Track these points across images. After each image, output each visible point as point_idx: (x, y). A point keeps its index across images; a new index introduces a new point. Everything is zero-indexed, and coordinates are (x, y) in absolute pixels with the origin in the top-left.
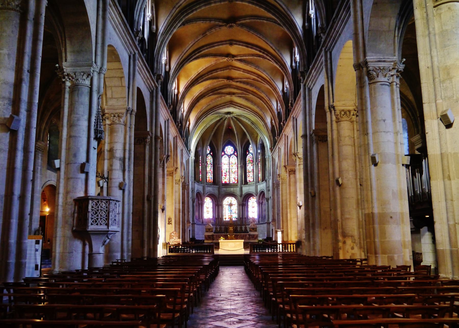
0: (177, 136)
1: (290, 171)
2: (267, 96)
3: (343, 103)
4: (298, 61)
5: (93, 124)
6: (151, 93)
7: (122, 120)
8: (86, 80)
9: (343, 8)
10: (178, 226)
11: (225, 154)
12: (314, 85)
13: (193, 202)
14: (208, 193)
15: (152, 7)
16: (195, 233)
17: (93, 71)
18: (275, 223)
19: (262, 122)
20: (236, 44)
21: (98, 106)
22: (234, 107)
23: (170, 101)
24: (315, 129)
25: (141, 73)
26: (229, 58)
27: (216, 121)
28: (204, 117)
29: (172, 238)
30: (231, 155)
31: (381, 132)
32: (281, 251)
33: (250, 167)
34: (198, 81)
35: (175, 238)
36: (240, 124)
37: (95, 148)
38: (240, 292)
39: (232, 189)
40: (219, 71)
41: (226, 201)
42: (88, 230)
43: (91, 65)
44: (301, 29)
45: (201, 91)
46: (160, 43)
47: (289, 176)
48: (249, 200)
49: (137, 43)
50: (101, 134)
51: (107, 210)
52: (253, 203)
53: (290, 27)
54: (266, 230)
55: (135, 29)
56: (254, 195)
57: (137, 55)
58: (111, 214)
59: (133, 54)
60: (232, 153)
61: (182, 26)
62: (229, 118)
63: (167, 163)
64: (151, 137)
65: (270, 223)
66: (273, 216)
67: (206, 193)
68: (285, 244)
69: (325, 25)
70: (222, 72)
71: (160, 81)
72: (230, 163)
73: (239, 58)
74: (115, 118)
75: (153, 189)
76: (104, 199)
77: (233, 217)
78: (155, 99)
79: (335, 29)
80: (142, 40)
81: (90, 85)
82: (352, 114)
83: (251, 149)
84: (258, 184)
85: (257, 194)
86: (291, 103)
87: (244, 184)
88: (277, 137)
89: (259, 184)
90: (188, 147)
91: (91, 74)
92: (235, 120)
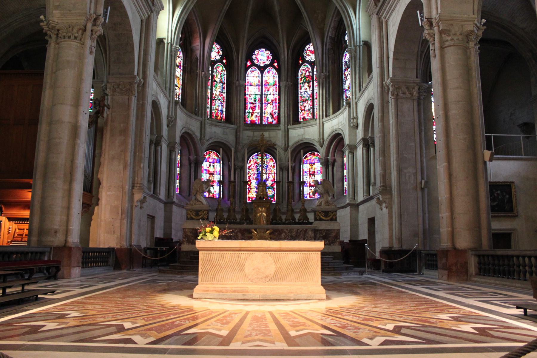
10: (66, 187)
11: (253, 64)
14: (211, 138)
16: (173, 225)
30: (266, 67)
33: (304, 90)
52: (312, 164)
54: (349, 224)
60: (268, 63)
65: (358, 205)
66: (385, 176)
72: (264, 83)
84: (325, 119)
85: (323, 141)
89: (328, 118)
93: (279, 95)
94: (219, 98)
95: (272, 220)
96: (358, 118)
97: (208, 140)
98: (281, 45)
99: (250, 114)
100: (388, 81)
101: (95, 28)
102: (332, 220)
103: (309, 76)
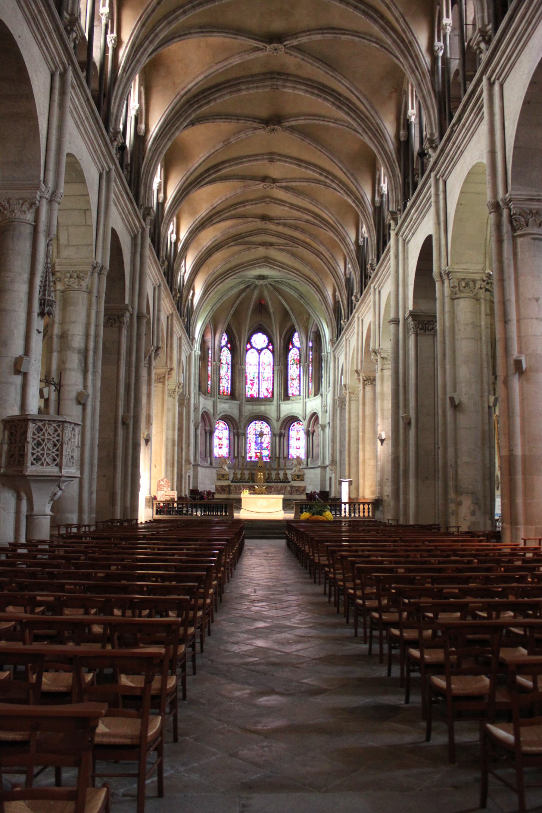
0: (172, 313)
1: (365, 379)
2: (328, 250)
3: (465, 267)
4: (386, 193)
5: (37, 289)
6: (134, 239)
7: (83, 284)
8: (27, 212)
9: (470, 107)
10: (171, 469)
11: (252, 347)
12: (413, 234)
13: (196, 429)
14: (221, 413)
15: (140, 93)
17: (40, 197)
18: (336, 468)
19: (319, 295)
20: (280, 160)
21: (47, 258)
22: (270, 267)
23: (163, 254)
24: (413, 308)
25: (118, 204)
26: (267, 184)
27: (239, 289)
28: (219, 282)
29: (161, 490)
30: (262, 349)
31: (532, 318)
32: (347, 515)
34: (212, 221)
35: (165, 489)
36: (280, 297)
37: (40, 330)
38: (286, 585)
39: (263, 408)
40: (249, 205)
41: (252, 429)
42: (26, 474)
43: (38, 188)
44: (393, 139)
45: (216, 238)
46: (151, 154)
47: (364, 388)
48: (291, 427)
49: (114, 152)
50: (51, 306)
51: (58, 441)
52: (298, 431)
53: (374, 135)
55: (111, 128)
56: (301, 419)
57: (113, 173)
58: (65, 446)
59: (106, 172)
60: (264, 345)
61: (190, 126)
62: (262, 285)
63: (156, 361)
64: (132, 315)
65: (326, 467)
67: (218, 413)
68: (352, 503)
69: (436, 135)
70: (254, 206)
71: (149, 219)
73: (284, 184)
74: (72, 279)
75: (132, 405)
76: (54, 421)
77: (263, 455)
78: (139, 249)
79: (454, 143)
80: (122, 148)
81: (34, 222)
82: (478, 286)
83: (297, 339)
86: (372, 265)
87: (284, 400)
88: (344, 322)
89: (309, 399)
90: (191, 334)
91: (37, 202)
92: (272, 289)
93: (273, 373)
94: (226, 377)
95: (267, 479)
96: (327, 406)
97: (219, 415)
98: (275, 333)
99: (250, 389)
100: (336, 397)
101: (179, 390)
102: (301, 480)
103: (297, 359)
